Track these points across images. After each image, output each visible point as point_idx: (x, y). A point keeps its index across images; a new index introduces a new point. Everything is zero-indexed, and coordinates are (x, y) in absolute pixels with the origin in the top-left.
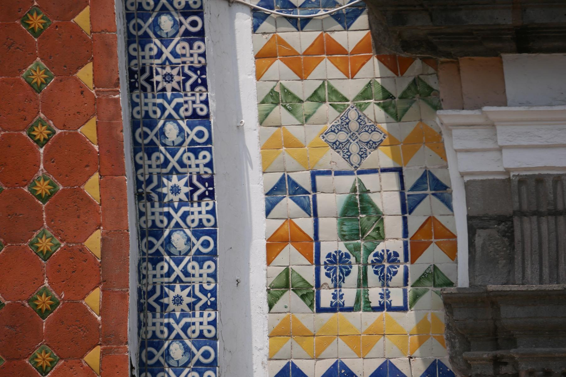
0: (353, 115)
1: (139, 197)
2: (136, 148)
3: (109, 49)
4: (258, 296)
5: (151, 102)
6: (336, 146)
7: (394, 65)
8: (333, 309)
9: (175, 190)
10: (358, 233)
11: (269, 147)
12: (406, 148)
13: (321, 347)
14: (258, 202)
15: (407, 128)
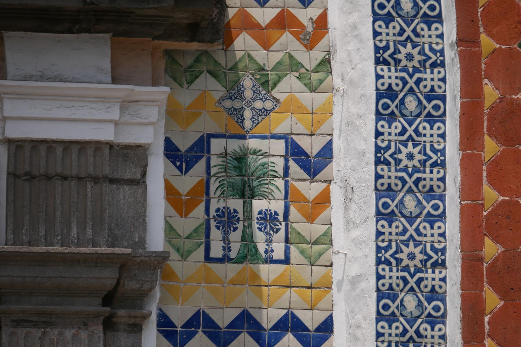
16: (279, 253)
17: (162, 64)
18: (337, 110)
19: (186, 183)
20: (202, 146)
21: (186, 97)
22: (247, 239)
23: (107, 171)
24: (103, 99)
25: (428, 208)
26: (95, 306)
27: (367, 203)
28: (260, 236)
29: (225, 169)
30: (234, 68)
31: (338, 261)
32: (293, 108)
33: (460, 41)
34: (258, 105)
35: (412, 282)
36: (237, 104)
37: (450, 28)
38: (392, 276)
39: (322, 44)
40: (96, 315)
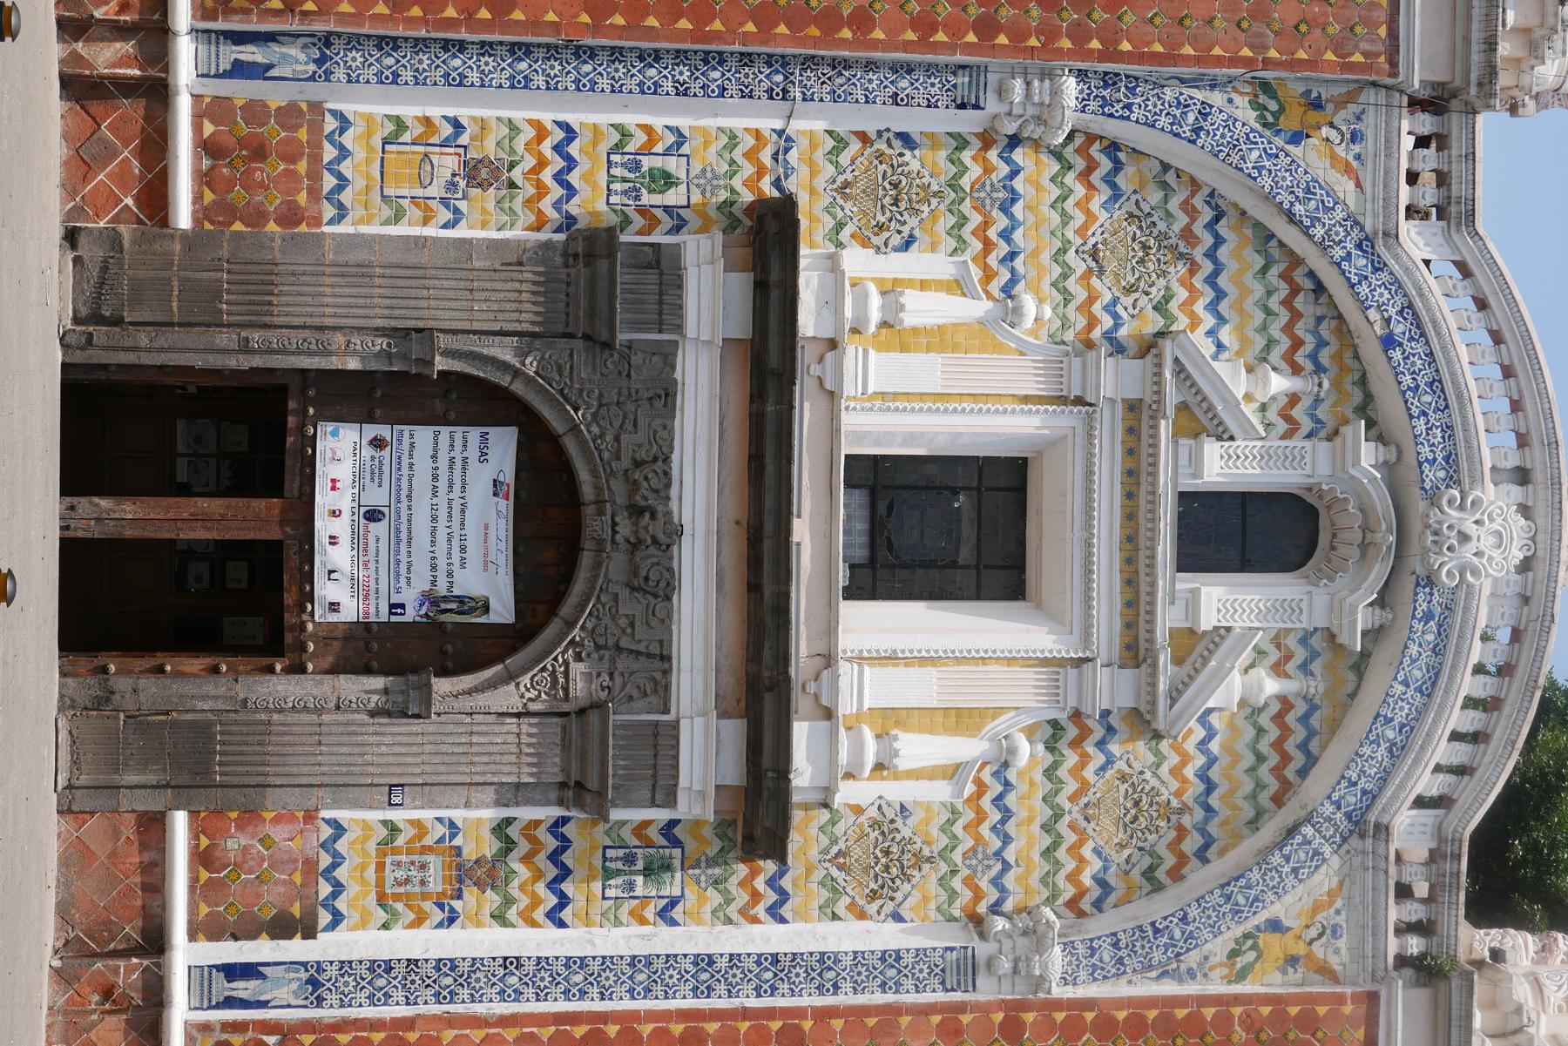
0: (722, 182)
1: (678, 51)
2: (707, 53)
3: (764, 43)
4: (618, 118)
5: (732, 63)
6: (704, 171)
7: (750, 209)
8: (609, 162)
9: (681, 73)
10: (651, 176)
11: (704, 131)
12: (701, 212)
13: (587, 153)
14: (673, 122)
15: (713, 213)
16: (609, 893)
17: (728, 817)
18: (700, 929)
19: (653, 833)
20: (676, 843)
21: (707, 832)
22: (618, 873)
23: (660, 783)
24: (705, 779)
25: (638, 989)
26: (575, 776)
27: (641, 949)
28: (619, 881)
29: (662, 858)
30: (726, 863)
31: (604, 931)
32: (702, 900)
33: (745, 1009)
34: (703, 878)
35: (591, 979)
36: (703, 865)
37: (753, 1002)
38: (595, 967)
39: (742, 920)
40: (569, 777)
